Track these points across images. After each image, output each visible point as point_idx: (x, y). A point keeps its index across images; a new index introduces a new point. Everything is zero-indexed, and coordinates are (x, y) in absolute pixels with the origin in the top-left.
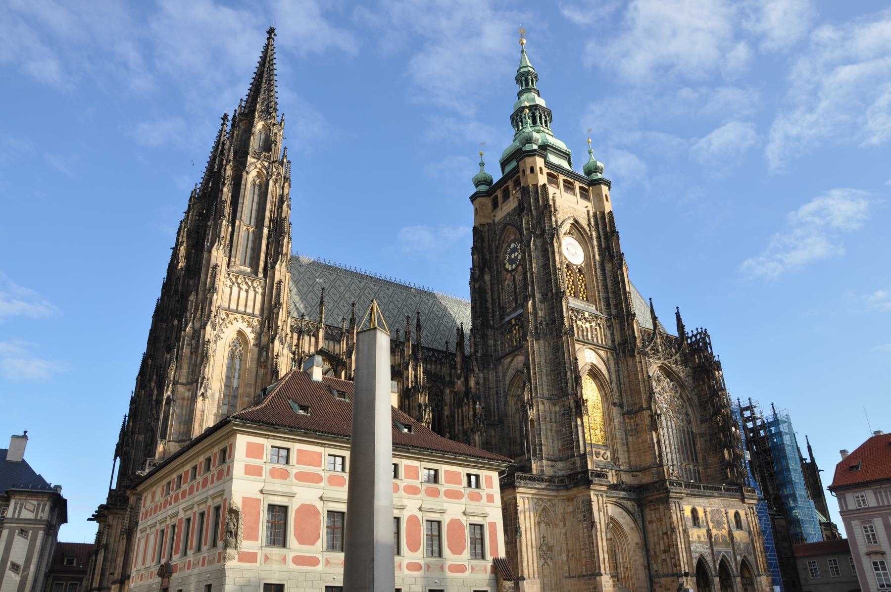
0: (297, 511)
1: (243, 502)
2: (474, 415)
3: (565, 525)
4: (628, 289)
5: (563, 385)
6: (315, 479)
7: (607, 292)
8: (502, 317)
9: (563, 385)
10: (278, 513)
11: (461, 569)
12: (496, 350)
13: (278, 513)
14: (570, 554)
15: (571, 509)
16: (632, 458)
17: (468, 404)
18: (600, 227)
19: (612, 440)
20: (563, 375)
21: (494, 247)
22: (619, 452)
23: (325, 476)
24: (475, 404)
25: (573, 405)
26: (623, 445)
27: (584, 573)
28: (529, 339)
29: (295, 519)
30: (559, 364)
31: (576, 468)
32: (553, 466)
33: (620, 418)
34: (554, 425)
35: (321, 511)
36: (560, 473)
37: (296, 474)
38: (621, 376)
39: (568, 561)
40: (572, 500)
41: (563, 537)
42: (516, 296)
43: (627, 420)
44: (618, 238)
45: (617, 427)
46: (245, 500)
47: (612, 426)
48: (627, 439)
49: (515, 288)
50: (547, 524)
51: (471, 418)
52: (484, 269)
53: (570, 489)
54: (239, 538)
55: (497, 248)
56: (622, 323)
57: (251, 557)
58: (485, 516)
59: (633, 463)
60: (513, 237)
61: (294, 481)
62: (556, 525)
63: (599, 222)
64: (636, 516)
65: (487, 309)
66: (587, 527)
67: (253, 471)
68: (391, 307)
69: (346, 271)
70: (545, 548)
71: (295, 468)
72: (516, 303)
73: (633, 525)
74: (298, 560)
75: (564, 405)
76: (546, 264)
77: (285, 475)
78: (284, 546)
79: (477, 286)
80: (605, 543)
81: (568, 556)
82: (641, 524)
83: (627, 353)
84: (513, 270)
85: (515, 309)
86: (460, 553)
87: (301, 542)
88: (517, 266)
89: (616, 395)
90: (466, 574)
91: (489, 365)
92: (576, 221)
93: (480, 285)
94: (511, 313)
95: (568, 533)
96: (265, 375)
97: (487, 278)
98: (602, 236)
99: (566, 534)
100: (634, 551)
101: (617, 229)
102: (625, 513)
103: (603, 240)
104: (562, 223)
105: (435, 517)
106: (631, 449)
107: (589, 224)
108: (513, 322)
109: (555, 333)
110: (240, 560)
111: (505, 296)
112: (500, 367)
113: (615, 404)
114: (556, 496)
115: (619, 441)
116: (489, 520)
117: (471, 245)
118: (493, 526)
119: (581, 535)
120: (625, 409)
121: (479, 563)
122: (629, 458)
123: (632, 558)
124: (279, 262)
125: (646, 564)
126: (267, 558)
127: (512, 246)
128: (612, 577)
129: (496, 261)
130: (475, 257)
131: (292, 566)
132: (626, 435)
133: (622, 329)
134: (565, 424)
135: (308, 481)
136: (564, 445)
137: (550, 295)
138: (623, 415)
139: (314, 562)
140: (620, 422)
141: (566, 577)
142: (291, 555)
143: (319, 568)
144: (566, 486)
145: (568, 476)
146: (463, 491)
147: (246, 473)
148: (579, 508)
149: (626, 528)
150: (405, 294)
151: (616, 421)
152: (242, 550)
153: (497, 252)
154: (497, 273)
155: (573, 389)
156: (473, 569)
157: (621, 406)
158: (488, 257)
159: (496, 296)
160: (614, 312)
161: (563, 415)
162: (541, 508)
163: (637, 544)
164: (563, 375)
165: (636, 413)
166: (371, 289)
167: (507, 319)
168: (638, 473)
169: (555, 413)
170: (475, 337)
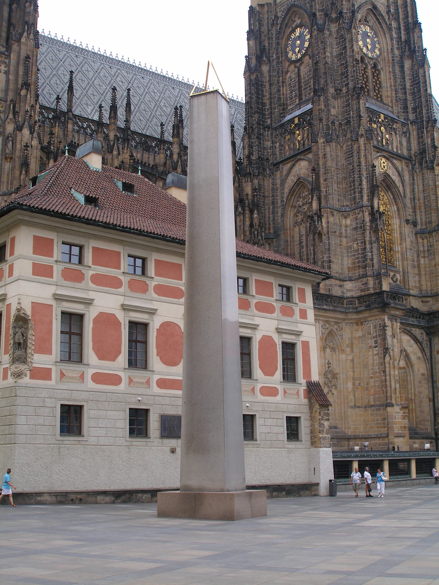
0: (96, 321)
1: (33, 308)
2: (251, 226)
3: (352, 351)
4: (429, 91)
5: (357, 195)
6: (114, 283)
7: (405, 93)
8: (282, 115)
9: (357, 195)
10: (73, 322)
11: (273, 392)
12: (274, 154)
13: (73, 322)
14: (357, 383)
15: (360, 334)
16: (424, 283)
17: (244, 214)
18: (401, 17)
19: (403, 261)
20: (357, 184)
21: (274, 32)
22: (410, 275)
24: (252, 212)
25: (367, 218)
26: (414, 267)
27: (372, 403)
28: (321, 141)
29: (93, 329)
30: (353, 170)
31: (368, 289)
32: (341, 286)
33: (413, 238)
34: (344, 240)
35: (122, 321)
36: (349, 294)
38: (416, 190)
39: (354, 390)
40: (362, 324)
41: (349, 364)
42: (300, 91)
43: (420, 241)
44: (421, 31)
45: (408, 247)
46: (35, 305)
47: (404, 245)
48: (418, 261)
49: (299, 82)
50: (333, 349)
51: (247, 229)
52: (261, 57)
53: (360, 312)
54: (29, 351)
55: (279, 33)
56: (420, 130)
57: (44, 374)
58: (298, 334)
59: (424, 288)
60: (298, 21)
62: (343, 351)
63: (400, 10)
64: (424, 345)
65: (264, 104)
66: (377, 354)
68: (147, 98)
69: (94, 53)
70: (329, 376)
72: (300, 99)
73: (420, 354)
74: (98, 378)
75: (356, 219)
76: (341, 54)
77: (78, 277)
78: (80, 361)
79: (253, 77)
80: (397, 372)
81: (354, 384)
82: (428, 354)
83: (424, 165)
84: (298, 61)
85: (299, 106)
86: (272, 374)
87: (101, 357)
88: (303, 56)
89: (410, 211)
90: (279, 398)
91: (264, 170)
92: (375, 7)
93: (257, 76)
94: (293, 110)
95: (356, 360)
96: (13, 168)
97: (265, 69)
98: (402, 28)
99: (353, 361)
100: (420, 382)
101: (420, 20)
102: (412, 342)
103: (403, 32)
104: (359, 7)
105: (246, 332)
106: (423, 272)
107: (388, 12)
108: (296, 121)
109: (349, 136)
110: (32, 377)
111: (286, 90)
112: (278, 173)
113: (407, 221)
114: (344, 320)
115: (410, 262)
116: (302, 338)
117: (247, 29)
118: (306, 345)
119: (370, 362)
120: (419, 227)
121: (289, 386)
122: (420, 281)
123: (417, 389)
124: (25, 34)
125: (431, 396)
126: (62, 375)
127: (298, 31)
128: (403, 408)
129: (277, 49)
130: (251, 43)
131: (91, 384)
132: (418, 256)
133: (420, 137)
134: (356, 240)
135: (106, 286)
136: (354, 263)
137: (344, 90)
138: (416, 234)
139: (115, 380)
140: (412, 242)
141: (352, 407)
142: (90, 372)
143: (122, 387)
144: (356, 308)
145: (359, 298)
146: (275, 304)
147: (34, 274)
148: (370, 333)
149: (413, 358)
150: (162, 85)
151: (408, 240)
152: (34, 365)
153: (278, 38)
154: (278, 63)
155: (368, 200)
156: (285, 392)
157: (415, 224)
158: (267, 45)
159: (274, 90)
160: (412, 117)
161: (356, 229)
162: (327, 331)
163: (423, 375)
164: (357, 184)
165: (430, 233)
166: (124, 76)
167: (288, 117)
168: (428, 299)
169: (346, 226)
170: (249, 138)
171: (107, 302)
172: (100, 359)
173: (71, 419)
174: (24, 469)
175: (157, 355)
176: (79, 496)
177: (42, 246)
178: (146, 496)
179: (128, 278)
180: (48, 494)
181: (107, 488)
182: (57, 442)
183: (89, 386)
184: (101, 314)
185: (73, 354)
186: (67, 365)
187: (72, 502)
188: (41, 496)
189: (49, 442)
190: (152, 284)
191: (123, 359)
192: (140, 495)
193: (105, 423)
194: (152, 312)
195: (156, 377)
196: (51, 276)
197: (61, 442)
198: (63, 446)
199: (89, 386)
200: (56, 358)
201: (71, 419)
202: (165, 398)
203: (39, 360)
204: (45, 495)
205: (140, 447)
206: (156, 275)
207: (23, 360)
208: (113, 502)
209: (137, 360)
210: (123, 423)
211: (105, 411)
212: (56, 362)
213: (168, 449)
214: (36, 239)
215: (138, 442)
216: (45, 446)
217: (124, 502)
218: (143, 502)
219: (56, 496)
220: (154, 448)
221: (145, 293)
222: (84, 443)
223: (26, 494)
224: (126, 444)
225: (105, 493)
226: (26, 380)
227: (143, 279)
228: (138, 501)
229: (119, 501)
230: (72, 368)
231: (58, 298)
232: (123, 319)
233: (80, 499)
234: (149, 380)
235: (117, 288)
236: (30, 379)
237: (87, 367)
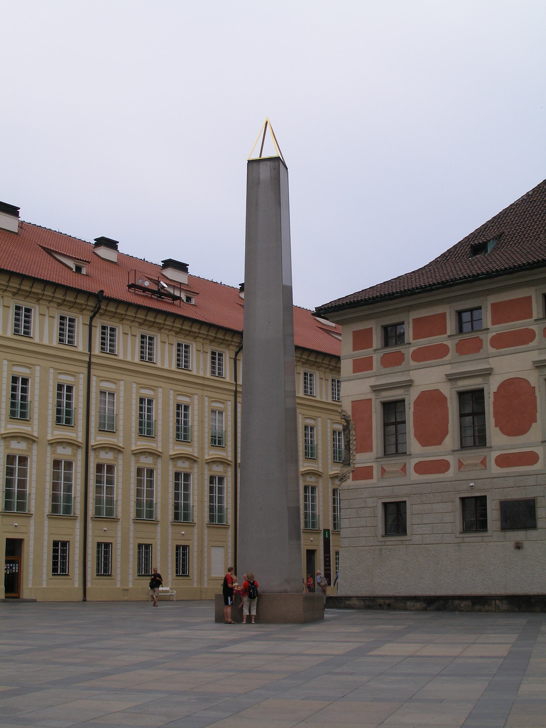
1: (353, 407)
23: (451, 344)
37: (414, 352)
46: (355, 403)
57: (365, 473)
61: (413, 363)
67: (362, 366)
71: (413, 343)
77: (398, 359)
126: (383, 471)
131: (414, 477)
142: (414, 461)
143: (451, 473)
171: (429, 378)
172: (423, 445)
173: (395, 518)
174: (347, 572)
175: (496, 426)
176: (387, 601)
177: (362, 340)
178: (463, 604)
179: (456, 340)
180: (356, 598)
181: (419, 593)
182: (379, 544)
183: (412, 479)
184: (423, 393)
185: (394, 447)
186: (396, 458)
187: (381, 607)
188: (349, 600)
189: (371, 544)
190: (487, 338)
191: (451, 440)
192: (457, 602)
193: (434, 517)
194: (487, 373)
195: (494, 454)
196: (370, 367)
197: (383, 543)
198: (384, 547)
199: (412, 479)
200: (377, 454)
201: (395, 518)
202: (508, 478)
203: (361, 459)
204: (353, 599)
205: (474, 544)
206: (493, 323)
207: (347, 463)
208: (425, 609)
209: (475, 437)
210: (453, 516)
211: (430, 505)
212: (377, 458)
213: (511, 545)
214: (356, 334)
215: (473, 537)
216: (367, 548)
217: (438, 609)
218: (461, 611)
219: (364, 600)
220: (492, 544)
221: (479, 352)
222: (407, 543)
223: (336, 597)
224: (458, 540)
225: (415, 598)
226: (350, 482)
227: (474, 335)
228: (455, 609)
229: (432, 608)
230: (393, 462)
231: (376, 389)
232: (449, 392)
233: (389, 605)
234: (485, 459)
235: (442, 358)
236: (353, 480)
237: (409, 457)
